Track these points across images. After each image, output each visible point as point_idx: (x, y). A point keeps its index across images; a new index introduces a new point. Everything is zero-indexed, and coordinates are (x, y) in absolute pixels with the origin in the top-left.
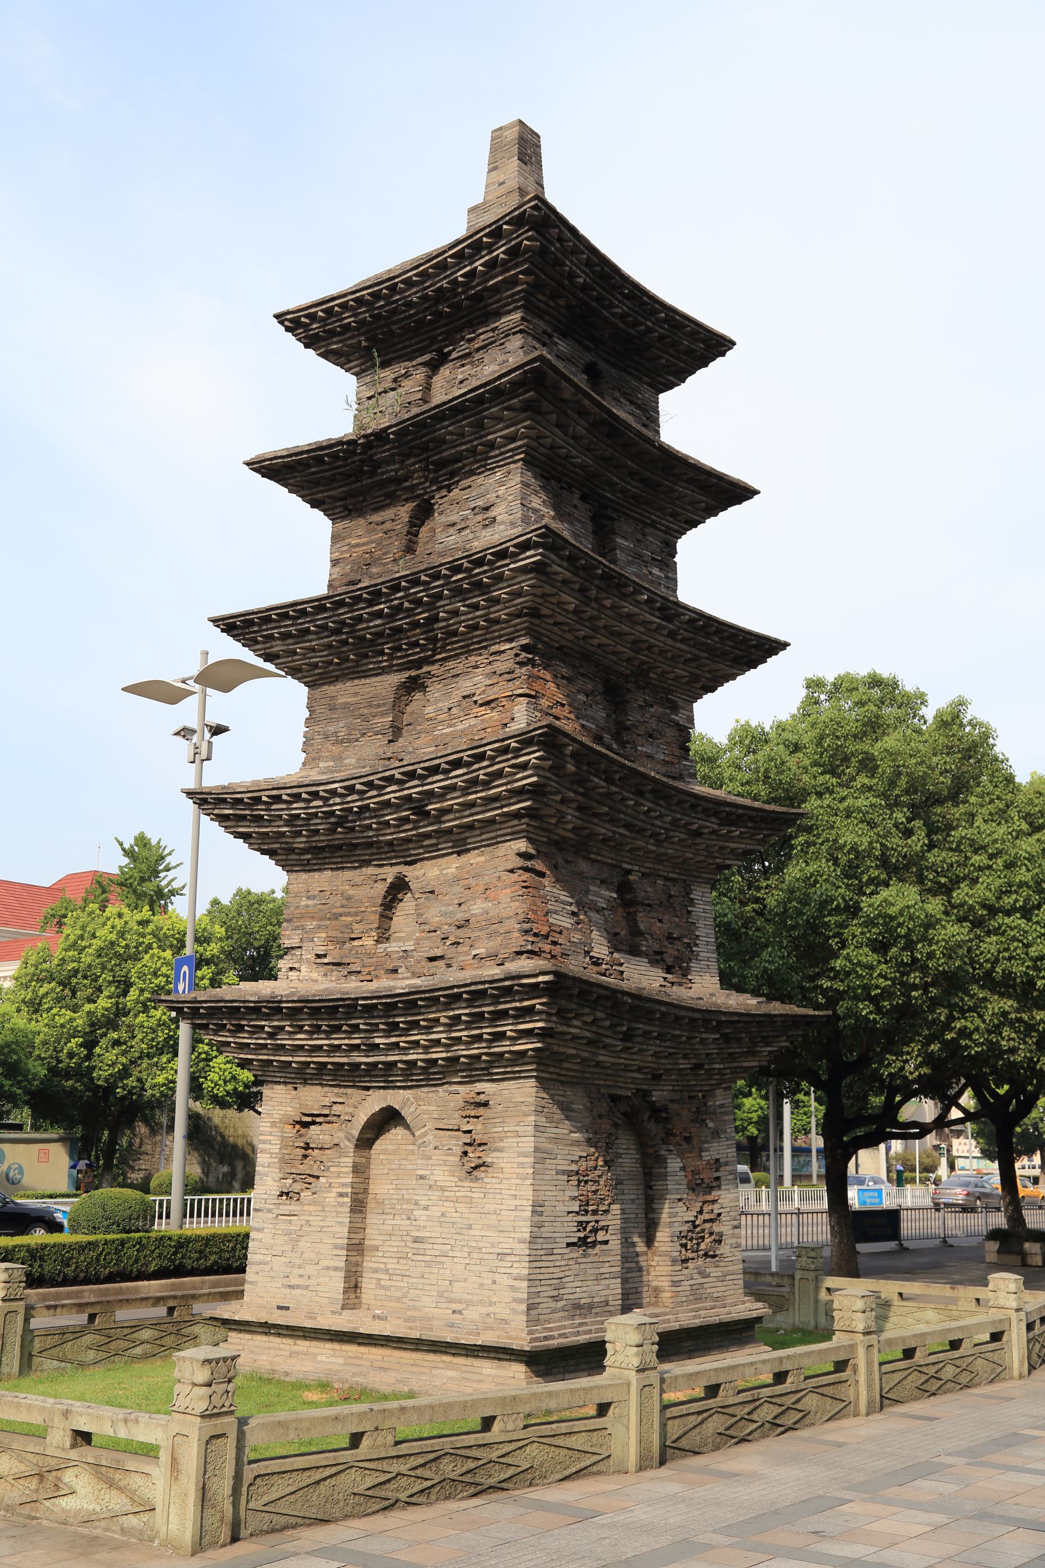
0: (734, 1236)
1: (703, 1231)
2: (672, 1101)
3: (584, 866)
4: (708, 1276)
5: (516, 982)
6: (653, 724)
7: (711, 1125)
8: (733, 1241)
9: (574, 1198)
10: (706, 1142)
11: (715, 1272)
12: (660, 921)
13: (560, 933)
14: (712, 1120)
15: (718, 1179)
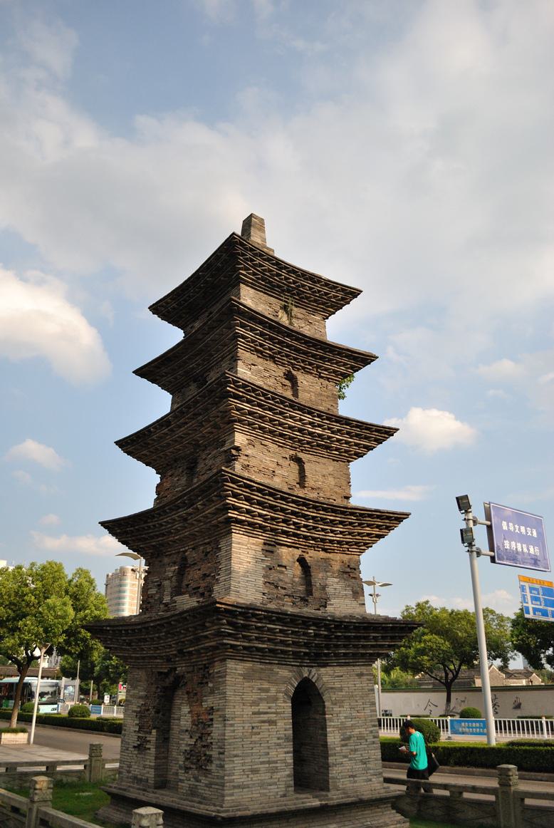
0: (219, 759)
1: (200, 752)
2: (188, 672)
3: (166, 560)
4: (200, 782)
5: (143, 626)
6: (210, 463)
7: (210, 685)
8: (218, 762)
9: (137, 724)
10: (205, 696)
11: (204, 780)
12: (199, 570)
13: (152, 597)
14: (211, 682)
15: (212, 720)
